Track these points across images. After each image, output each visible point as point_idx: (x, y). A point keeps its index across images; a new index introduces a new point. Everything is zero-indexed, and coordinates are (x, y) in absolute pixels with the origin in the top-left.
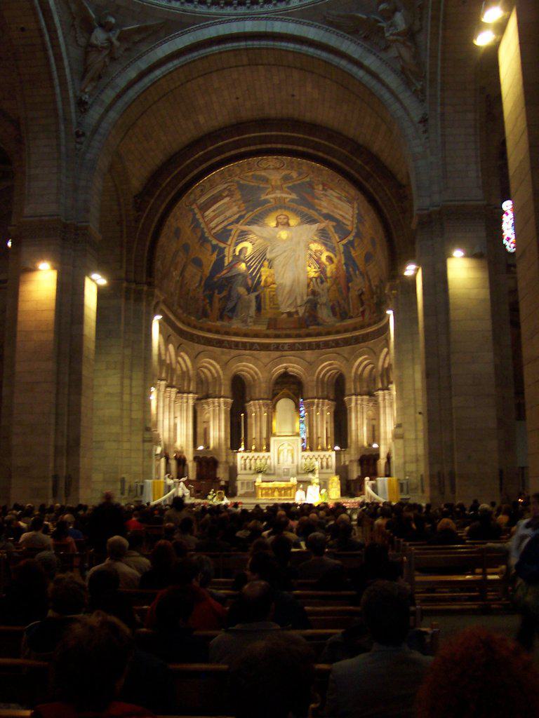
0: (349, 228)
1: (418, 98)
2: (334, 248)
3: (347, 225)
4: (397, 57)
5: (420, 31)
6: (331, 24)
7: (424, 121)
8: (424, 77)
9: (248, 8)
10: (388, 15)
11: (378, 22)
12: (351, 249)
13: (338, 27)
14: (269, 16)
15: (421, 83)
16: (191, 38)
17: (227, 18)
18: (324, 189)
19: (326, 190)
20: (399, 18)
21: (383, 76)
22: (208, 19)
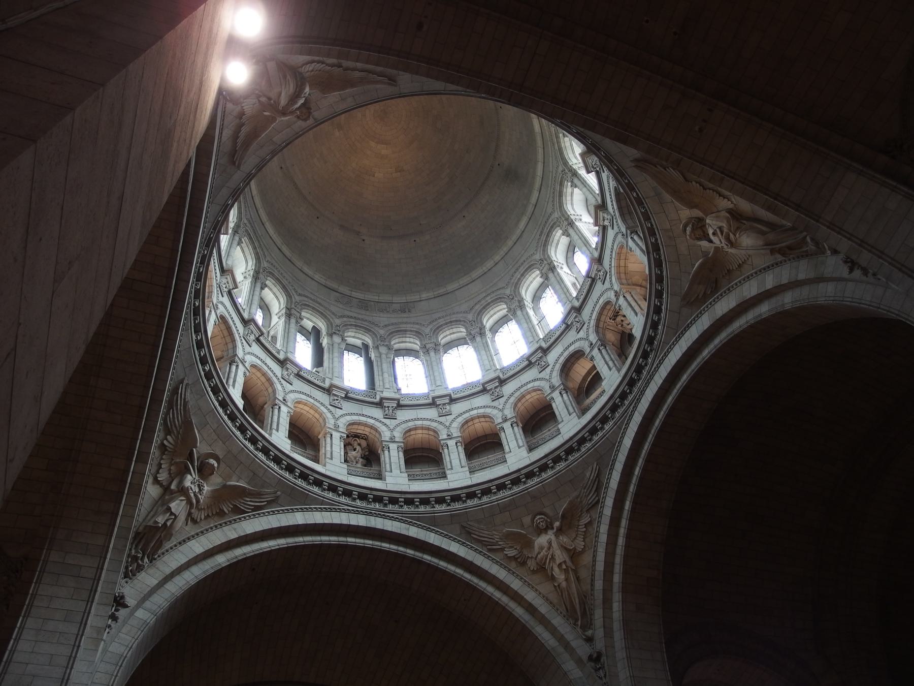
4: (172, 514)
5: (195, 522)
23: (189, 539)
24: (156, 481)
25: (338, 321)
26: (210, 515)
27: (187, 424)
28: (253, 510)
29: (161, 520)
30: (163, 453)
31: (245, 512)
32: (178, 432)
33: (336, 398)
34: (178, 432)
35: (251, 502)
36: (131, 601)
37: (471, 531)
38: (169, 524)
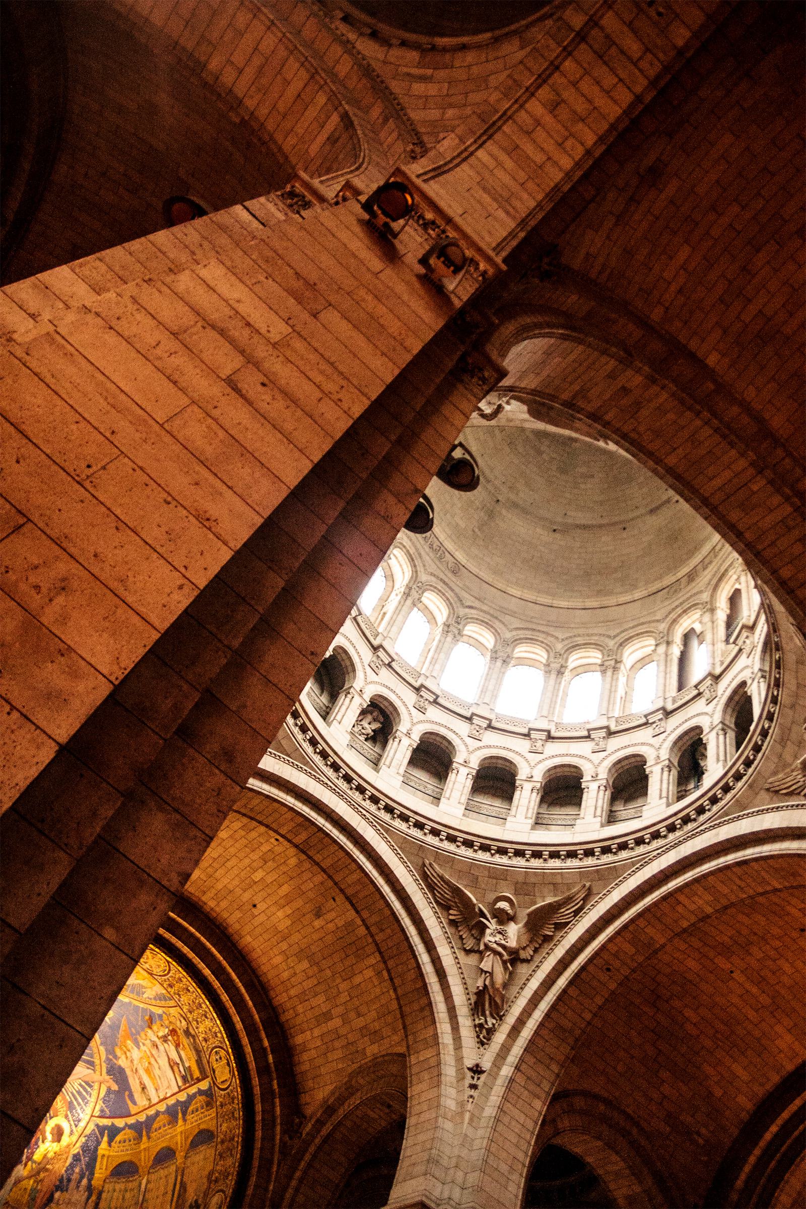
0: (133, 1109)
1: (478, 1037)
2: (79, 1121)
3: (135, 1103)
4: (486, 972)
5: (527, 961)
6: (425, 877)
7: (477, 1070)
8: (501, 1018)
9: (351, 789)
10: (504, 918)
11: (482, 915)
12: (105, 1139)
13: (431, 887)
14: (368, 815)
15: (494, 1021)
16: (277, 767)
17: (326, 780)
18: (165, 1039)
19: (165, 1041)
20: (513, 930)
21: (450, 979)
22: (306, 764)
23: (528, 980)
24: (468, 952)
25: (663, 627)
26: (537, 946)
27: (457, 891)
28: (575, 916)
29: (480, 983)
30: (457, 927)
31: (568, 923)
32: (455, 902)
33: (654, 725)
34: (455, 902)
35: (567, 911)
36: (486, 1065)
37: (777, 788)
38: (487, 983)
